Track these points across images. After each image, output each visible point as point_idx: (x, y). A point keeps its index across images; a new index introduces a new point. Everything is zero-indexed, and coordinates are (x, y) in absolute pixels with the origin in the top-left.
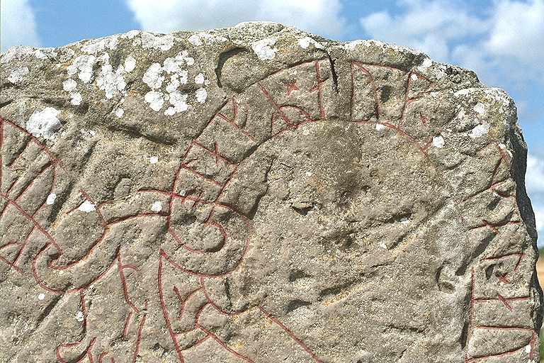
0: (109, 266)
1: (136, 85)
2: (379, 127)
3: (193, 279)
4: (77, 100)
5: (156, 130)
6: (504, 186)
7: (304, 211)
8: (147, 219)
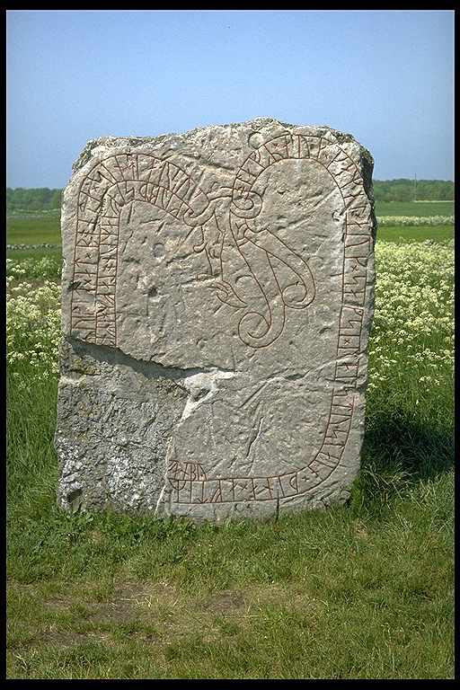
2: (310, 160)
3: (242, 220)
5: (226, 164)
6: (357, 181)
7: (282, 193)
8: (224, 199)
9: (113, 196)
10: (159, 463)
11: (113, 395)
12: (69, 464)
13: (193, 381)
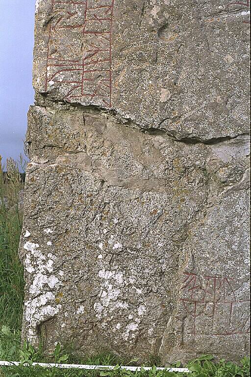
10: (166, 279)
11: (103, 182)
12: (40, 280)
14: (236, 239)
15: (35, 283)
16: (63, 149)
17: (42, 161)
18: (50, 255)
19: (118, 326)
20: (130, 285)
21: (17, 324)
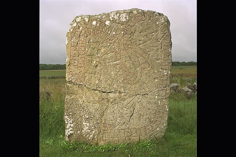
0: (117, 40)
1: (119, 17)
4: (112, 20)
9: (83, 34)
11: (84, 101)
13: (111, 95)
14: (115, 115)
15: (68, 125)
16: (74, 94)
17: (69, 97)
18: (71, 119)
19: (88, 136)
20: (91, 126)
21: (64, 135)
